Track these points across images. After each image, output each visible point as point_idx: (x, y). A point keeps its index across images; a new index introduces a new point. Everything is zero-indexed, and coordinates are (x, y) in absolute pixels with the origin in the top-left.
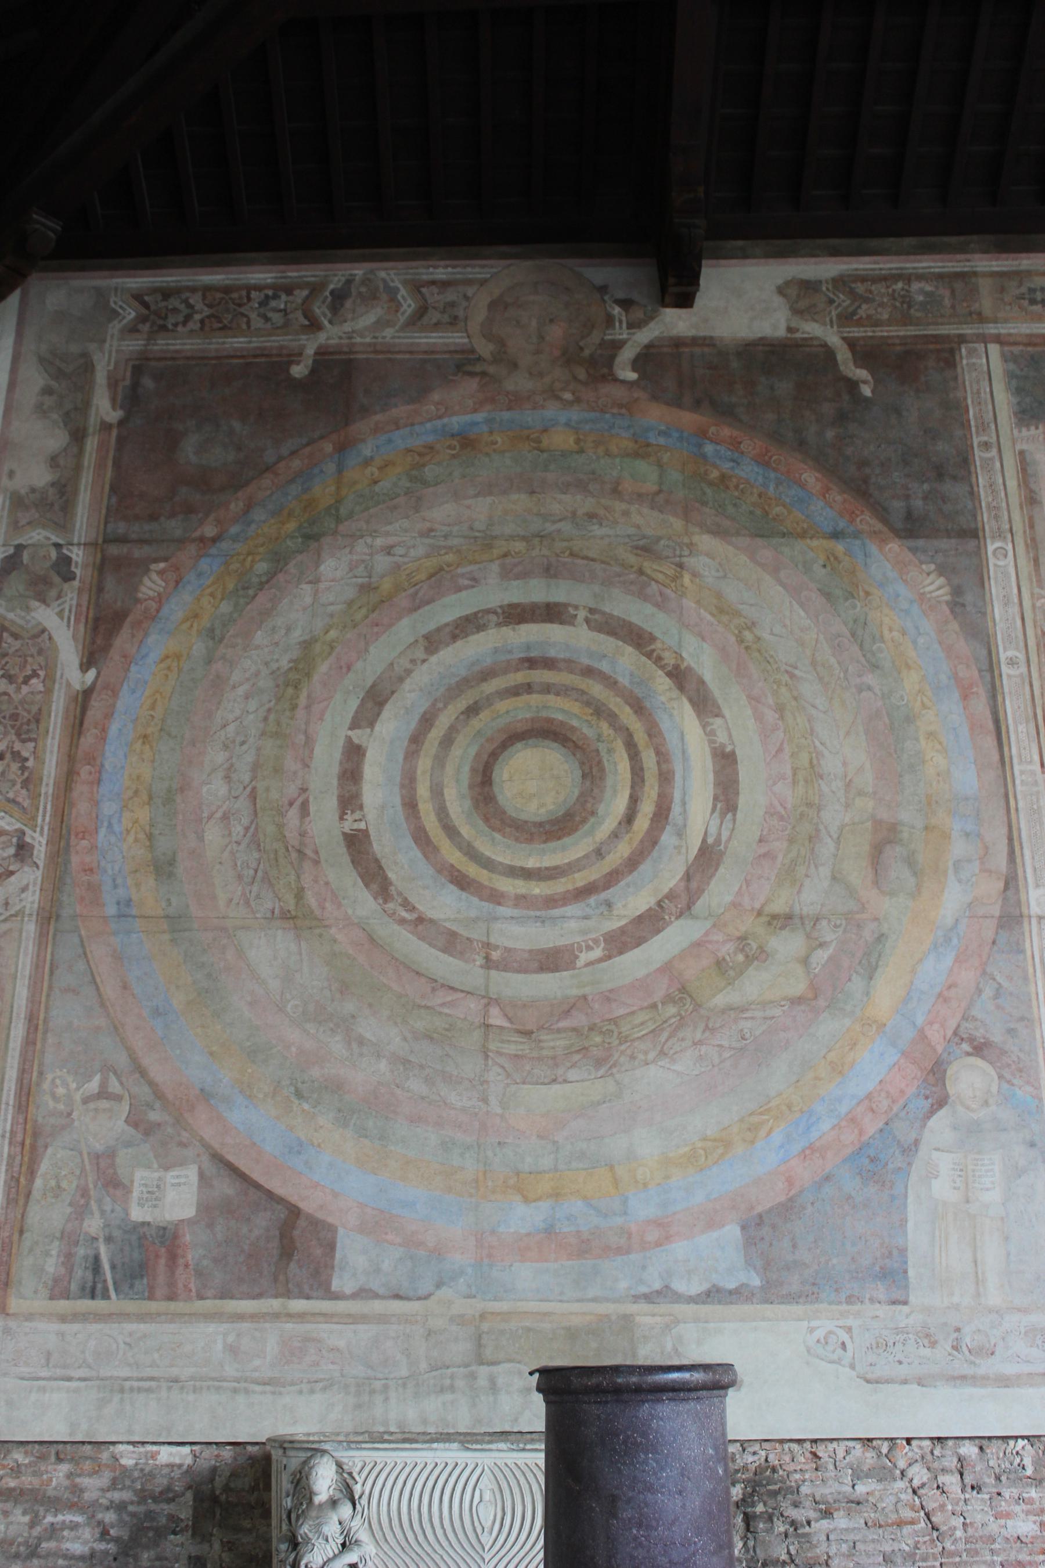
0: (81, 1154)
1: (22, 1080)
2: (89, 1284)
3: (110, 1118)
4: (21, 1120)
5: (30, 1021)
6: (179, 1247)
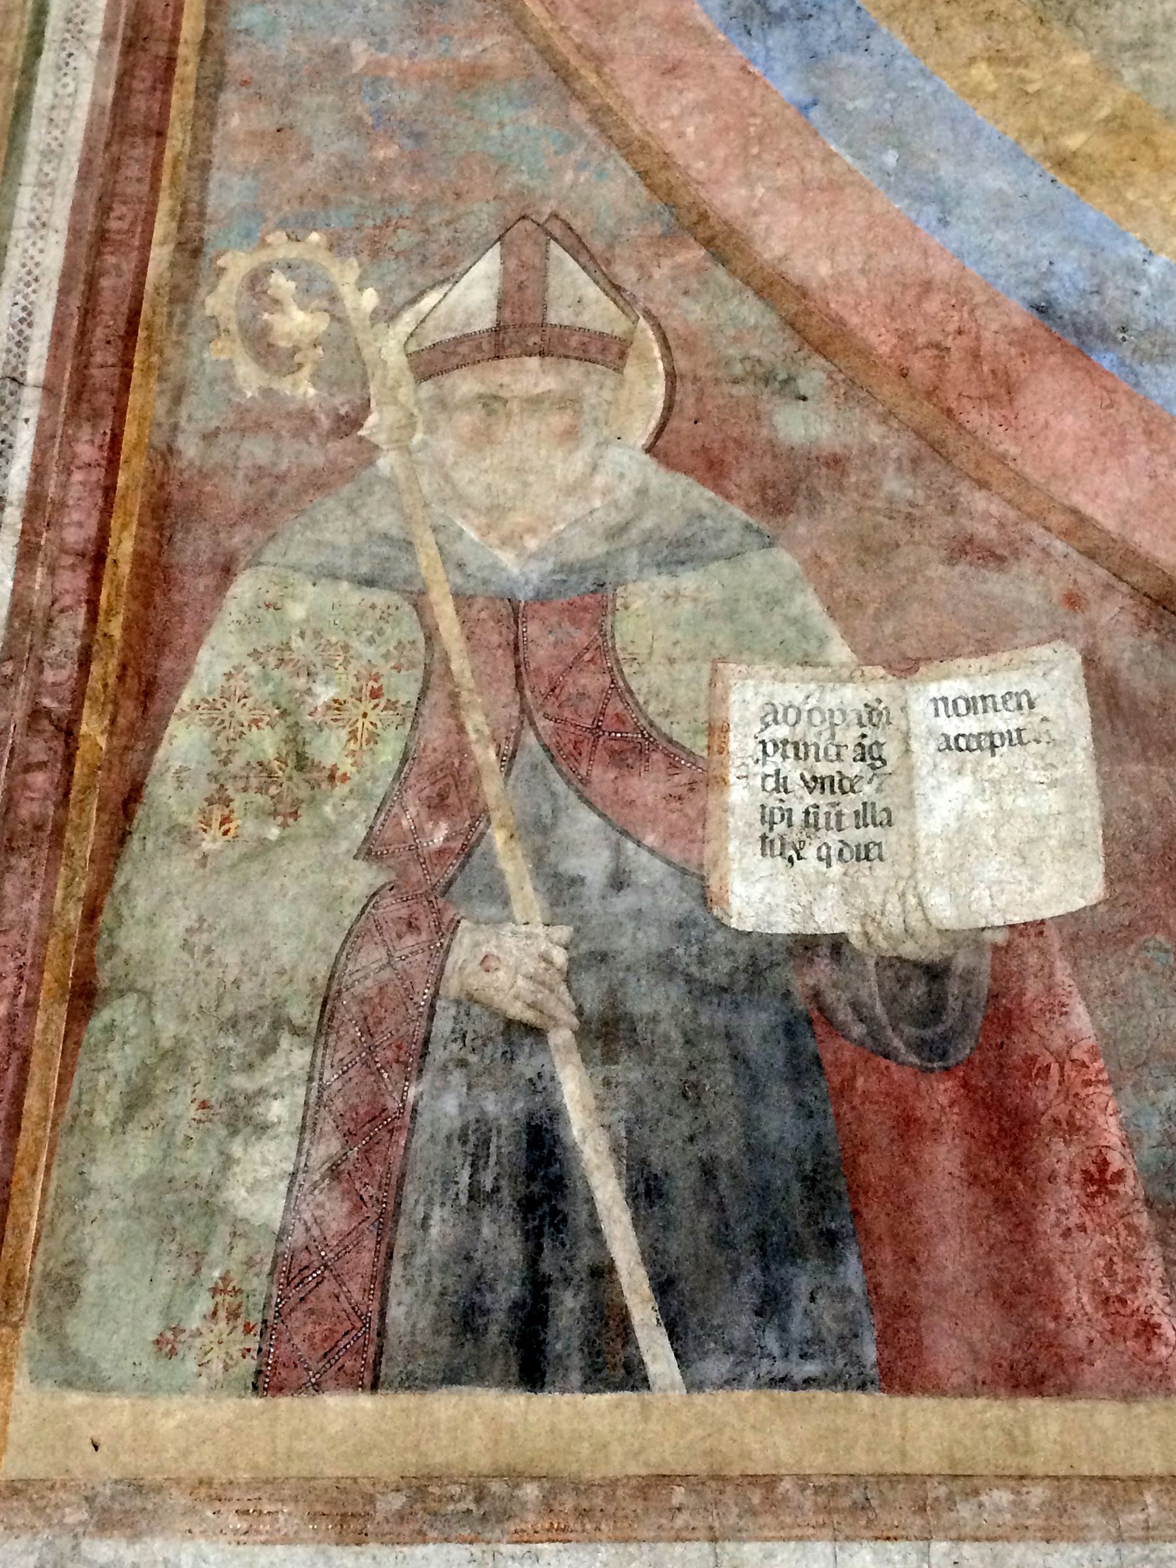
0: (419, 602)
1: (92, 282)
2: (507, 1292)
3: (571, 435)
4: (86, 451)
5: (129, 46)
6: (1033, 1070)
